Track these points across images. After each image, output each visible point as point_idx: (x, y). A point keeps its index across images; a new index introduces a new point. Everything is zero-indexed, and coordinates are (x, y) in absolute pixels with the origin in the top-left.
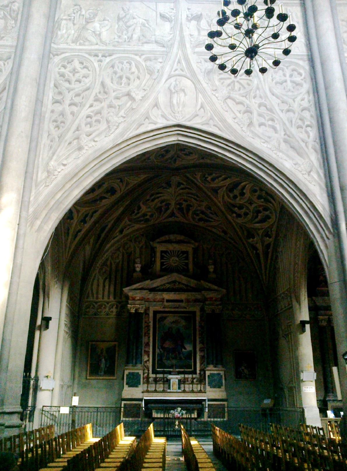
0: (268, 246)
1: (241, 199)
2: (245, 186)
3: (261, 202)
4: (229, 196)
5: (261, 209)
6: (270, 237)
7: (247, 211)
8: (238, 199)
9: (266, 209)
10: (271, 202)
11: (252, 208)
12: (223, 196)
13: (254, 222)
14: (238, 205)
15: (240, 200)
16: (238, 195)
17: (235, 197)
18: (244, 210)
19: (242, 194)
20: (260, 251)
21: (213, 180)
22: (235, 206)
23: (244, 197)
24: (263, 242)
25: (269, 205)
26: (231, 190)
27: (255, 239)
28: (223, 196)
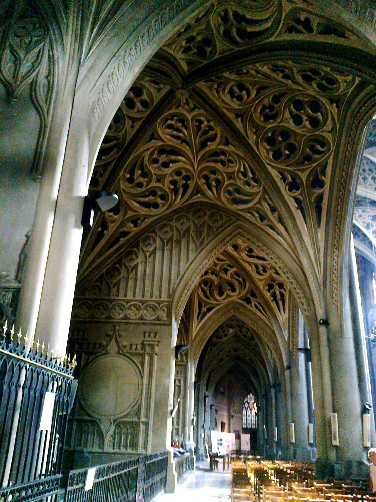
0: (125, 234)
1: (158, 168)
2: (178, 161)
3: (167, 186)
4: (152, 154)
5: (159, 193)
6: (136, 226)
7: (145, 183)
8: (156, 165)
9: (163, 197)
10: (176, 194)
11: (154, 184)
12: (148, 149)
13: (134, 198)
14: (146, 170)
15: (155, 168)
16: (161, 162)
17: (156, 161)
18: (141, 179)
19: (166, 165)
20: (107, 234)
21: (170, 127)
22: (142, 168)
23: (163, 169)
24: (122, 224)
25: (172, 197)
26: (162, 151)
27: (116, 216)
28: (148, 149)
